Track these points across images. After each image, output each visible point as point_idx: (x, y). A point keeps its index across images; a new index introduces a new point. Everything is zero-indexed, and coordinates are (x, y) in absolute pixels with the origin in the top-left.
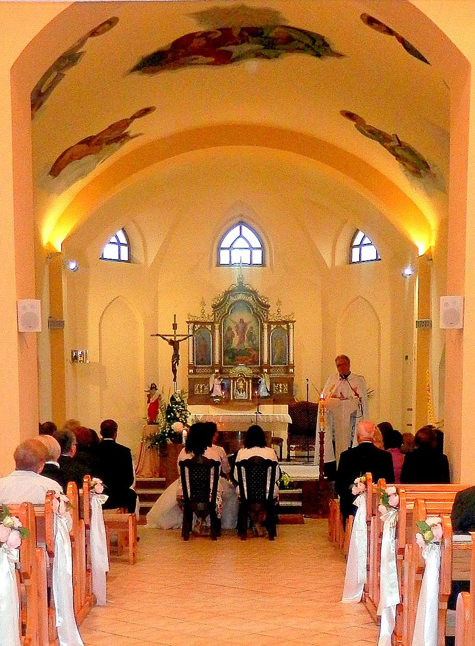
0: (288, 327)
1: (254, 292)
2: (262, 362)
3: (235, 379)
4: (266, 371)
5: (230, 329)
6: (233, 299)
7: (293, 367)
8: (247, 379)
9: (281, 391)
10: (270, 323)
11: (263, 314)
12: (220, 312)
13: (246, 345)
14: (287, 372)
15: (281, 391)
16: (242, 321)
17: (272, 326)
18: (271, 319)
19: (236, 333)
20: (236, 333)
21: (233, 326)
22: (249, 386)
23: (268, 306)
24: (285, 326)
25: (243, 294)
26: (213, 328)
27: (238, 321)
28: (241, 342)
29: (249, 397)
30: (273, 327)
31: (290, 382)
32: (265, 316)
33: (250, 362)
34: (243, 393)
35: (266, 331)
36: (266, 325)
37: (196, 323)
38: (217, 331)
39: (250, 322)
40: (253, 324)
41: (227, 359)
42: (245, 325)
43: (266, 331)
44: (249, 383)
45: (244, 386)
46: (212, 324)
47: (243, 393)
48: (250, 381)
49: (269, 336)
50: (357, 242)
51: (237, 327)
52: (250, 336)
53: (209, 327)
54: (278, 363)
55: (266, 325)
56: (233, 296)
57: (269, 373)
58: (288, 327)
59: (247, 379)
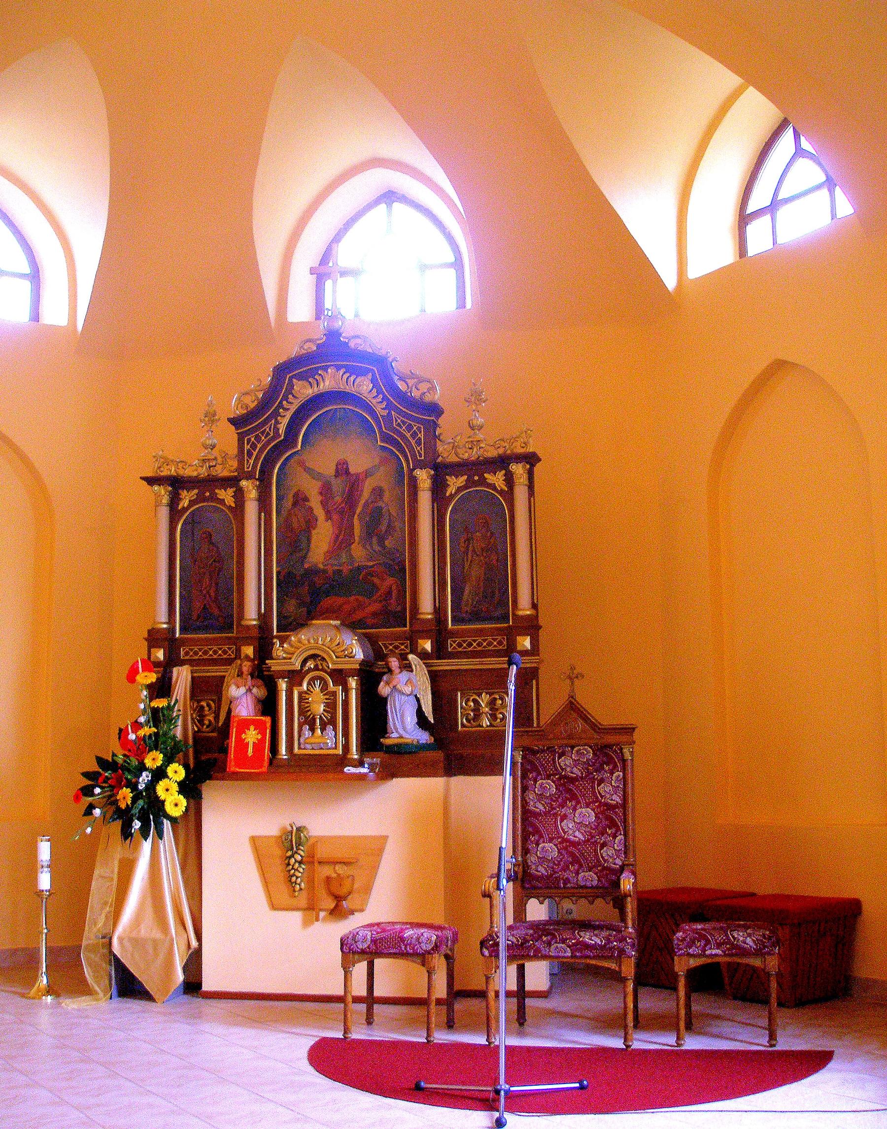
3: (295, 677)
4: (428, 646)
5: (300, 499)
6: (304, 391)
7: (532, 626)
9: (486, 722)
11: (414, 435)
12: (258, 438)
13: (359, 553)
15: (486, 722)
16: (342, 469)
19: (319, 512)
20: (319, 512)
21: (312, 490)
22: (346, 703)
24: (497, 479)
26: (240, 495)
27: (328, 469)
28: (342, 541)
29: (346, 748)
30: (454, 483)
32: (419, 442)
33: (374, 614)
34: (323, 729)
35: (425, 499)
37: (177, 483)
38: (251, 509)
39: (367, 474)
40: (382, 478)
41: (292, 606)
42: (354, 484)
44: (346, 690)
45: (331, 706)
46: (231, 482)
47: (323, 729)
48: (353, 683)
51: (326, 491)
52: (375, 517)
53: (227, 495)
54: (476, 616)
55: (424, 477)
56: (301, 377)
57: (440, 651)
58: (510, 479)
59: (340, 676)
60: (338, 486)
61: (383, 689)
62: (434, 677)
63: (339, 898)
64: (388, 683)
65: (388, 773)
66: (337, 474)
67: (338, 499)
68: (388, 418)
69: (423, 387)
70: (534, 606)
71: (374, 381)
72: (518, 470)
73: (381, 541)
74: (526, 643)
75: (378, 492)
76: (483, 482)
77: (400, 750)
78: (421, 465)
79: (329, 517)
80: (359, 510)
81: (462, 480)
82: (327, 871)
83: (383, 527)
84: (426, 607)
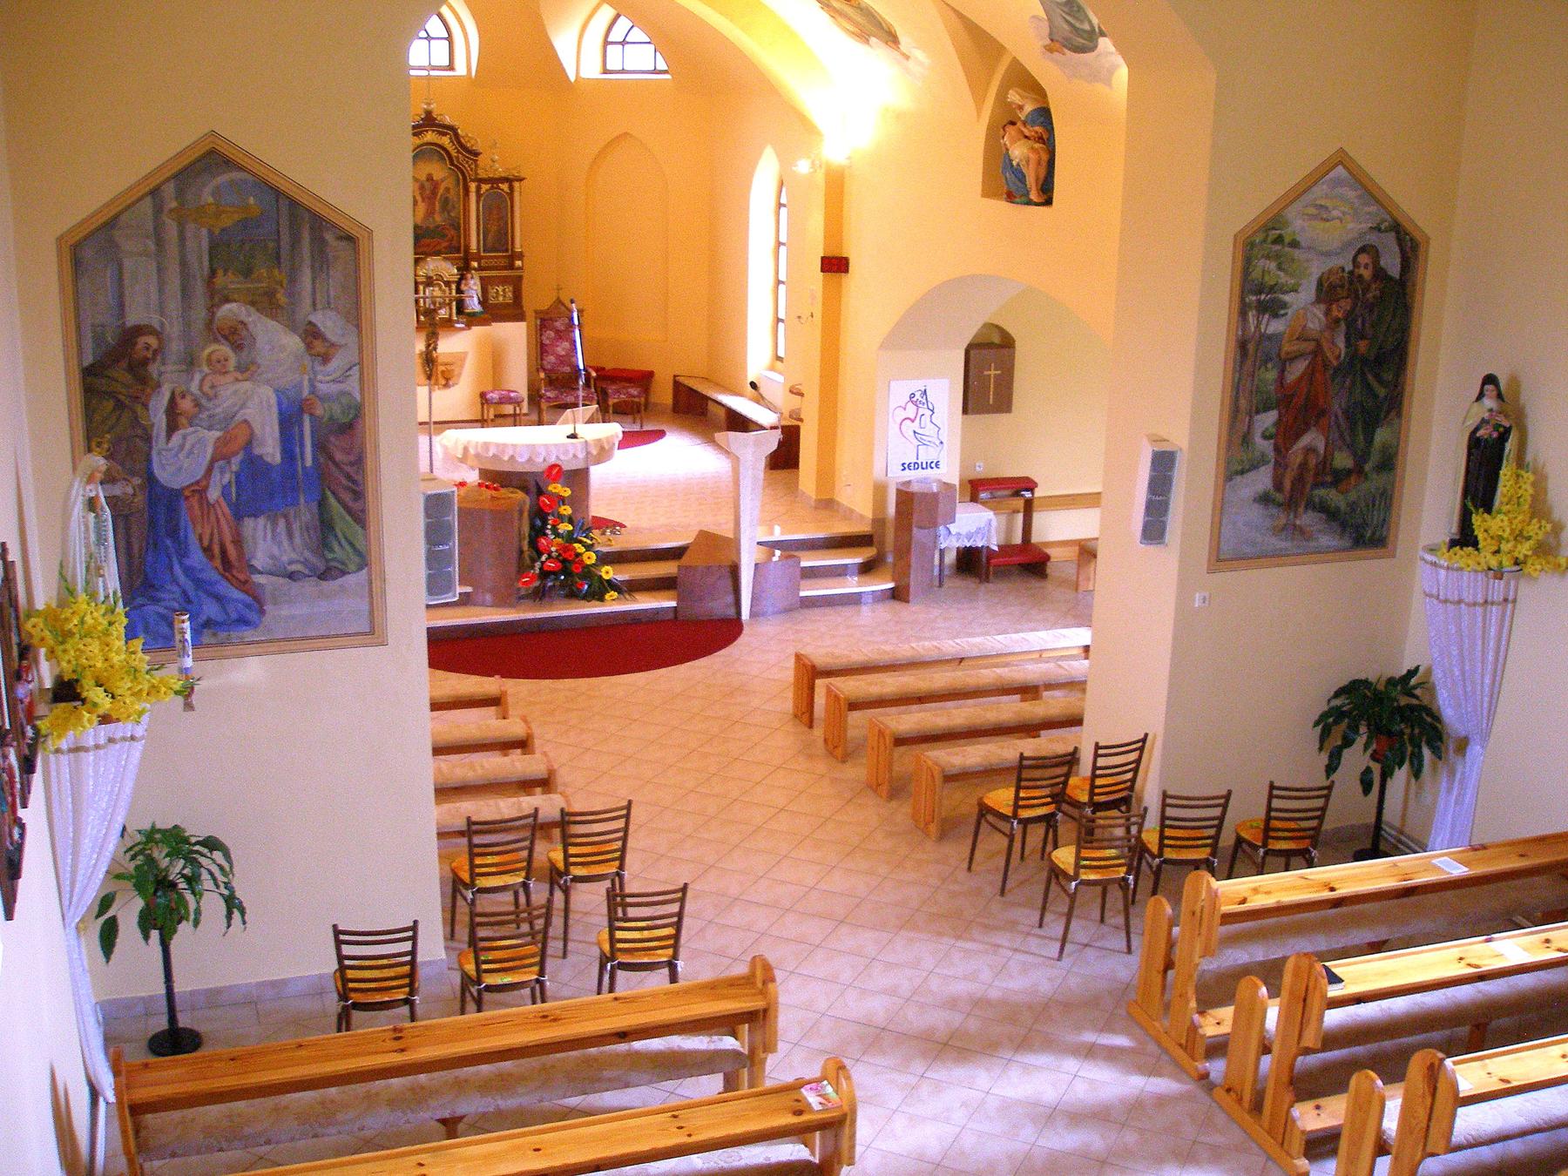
0: (511, 188)
1: (453, 129)
2: (467, 247)
8: (448, 284)
9: (501, 299)
10: (481, 181)
14: (511, 267)
15: (501, 299)
16: (430, 178)
17: (483, 186)
18: (482, 174)
23: (477, 154)
24: (505, 187)
25: (433, 131)
27: (424, 178)
29: (451, 315)
31: (517, 284)
33: (445, 248)
35: (473, 197)
36: (473, 186)
40: (449, 183)
43: (473, 197)
44: (450, 290)
49: (478, 202)
50: (617, 35)
52: (446, 201)
59: (448, 284)
60: (427, 185)
61: (463, 287)
62: (482, 279)
63: (447, 380)
64: (466, 285)
65: (469, 326)
66: (428, 180)
67: (428, 192)
68: (457, 158)
69: (473, 142)
70: (521, 247)
71: (451, 138)
72: (516, 184)
73: (448, 213)
74: (518, 263)
75: (447, 190)
76: (498, 188)
77: (473, 314)
78: (473, 181)
79: (423, 200)
80: (438, 197)
81: (488, 186)
82: (443, 368)
83: (450, 207)
84: (473, 247)
